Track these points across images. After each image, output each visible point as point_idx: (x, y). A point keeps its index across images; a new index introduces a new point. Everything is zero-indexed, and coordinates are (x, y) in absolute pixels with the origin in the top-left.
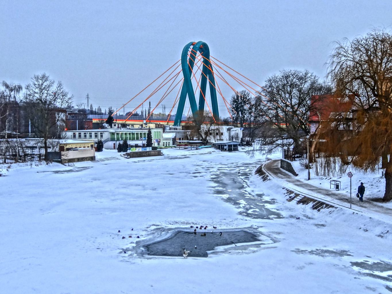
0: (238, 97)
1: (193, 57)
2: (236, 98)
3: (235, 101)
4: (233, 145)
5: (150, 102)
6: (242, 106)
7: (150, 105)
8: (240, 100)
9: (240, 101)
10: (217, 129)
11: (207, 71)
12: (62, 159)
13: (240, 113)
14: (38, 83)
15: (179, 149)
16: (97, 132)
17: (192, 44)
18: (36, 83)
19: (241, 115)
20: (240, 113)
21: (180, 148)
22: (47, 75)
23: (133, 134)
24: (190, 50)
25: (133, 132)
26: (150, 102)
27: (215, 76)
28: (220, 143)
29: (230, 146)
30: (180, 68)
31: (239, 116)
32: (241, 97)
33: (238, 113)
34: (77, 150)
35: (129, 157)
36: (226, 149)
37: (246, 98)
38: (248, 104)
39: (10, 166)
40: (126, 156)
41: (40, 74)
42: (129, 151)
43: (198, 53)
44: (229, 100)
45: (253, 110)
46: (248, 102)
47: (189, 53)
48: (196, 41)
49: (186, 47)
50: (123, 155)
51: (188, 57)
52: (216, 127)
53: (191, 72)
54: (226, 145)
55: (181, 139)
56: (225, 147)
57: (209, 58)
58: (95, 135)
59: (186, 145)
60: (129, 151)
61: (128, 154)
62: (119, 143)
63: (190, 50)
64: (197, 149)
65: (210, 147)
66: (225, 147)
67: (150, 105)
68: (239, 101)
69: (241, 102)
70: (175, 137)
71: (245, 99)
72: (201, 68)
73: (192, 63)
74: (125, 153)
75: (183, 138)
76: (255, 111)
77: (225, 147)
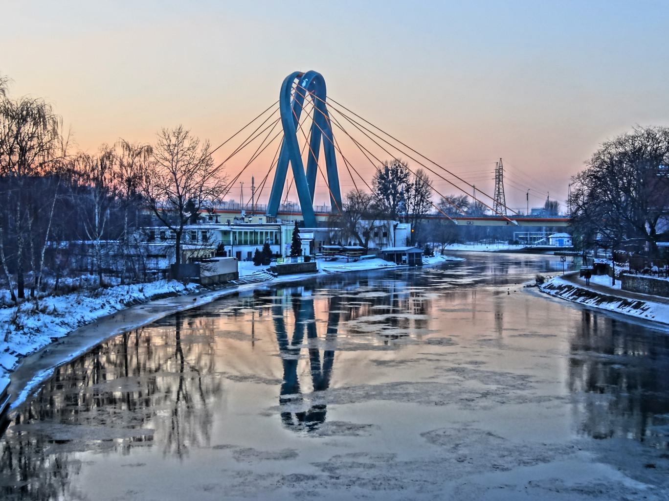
0: (387, 170)
1: (300, 98)
2: (383, 172)
3: (382, 177)
4: (417, 254)
5: (253, 178)
6: (395, 187)
7: (253, 183)
8: (390, 174)
9: (391, 178)
10: (384, 226)
11: (321, 122)
12: (202, 276)
13: (391, 197)
14: (169, 142)
15: (326, 261)
16: (197, 230)
17: (298, 75)
18: (165, 142)
19: (392, 203)
20: (391, 197)
21: (327, 259)
22: (184, 130)
23: (256, 233)
24: (294, 86)
25: (256, 231)
26: (253, 178)
27: (335, 130)
28: (395, 251)
29: (411, 255)
30: (278, 115)
31: (390, 204)
32: (393, 170)
33: (388, 199)
34: (218, 261)
35: (276, 274)
36: (405, 261)
37: (402, 172)
38: (404, 182)
39: (142, 289)
40: (271, 273)
41: (172, 127)
42: (273, 264)
43: (307, 93)
44: (371, 175)
45: (413, 192)
46: (404, 179)
47: (293, 92)
48: (304, 70)
49: (287, 81)
50: (267, 270)
51: (292, 98)
52: (382, 222)
53: (296, 123)
54: (405, 255)
55: (322, 243)
56: (403, 257)
57: (325, 101)
58: (193, 236)
59: (334, 254)
60: (273, 264)
61: (273, 269)
62: (257, 250)
63: (294, 86)
64: (355, 261)
65: (373, 258)
66: (404, 258)
67: (253, 183)
68: (388, 177)
69: (393, 179)
70: (314, 239)
71: (399, 174)
72: (312, 115)
73: (298, 108)
74: (268, 267)
75: (324, 242)
76: (415, 196)
77: (403, 257)
